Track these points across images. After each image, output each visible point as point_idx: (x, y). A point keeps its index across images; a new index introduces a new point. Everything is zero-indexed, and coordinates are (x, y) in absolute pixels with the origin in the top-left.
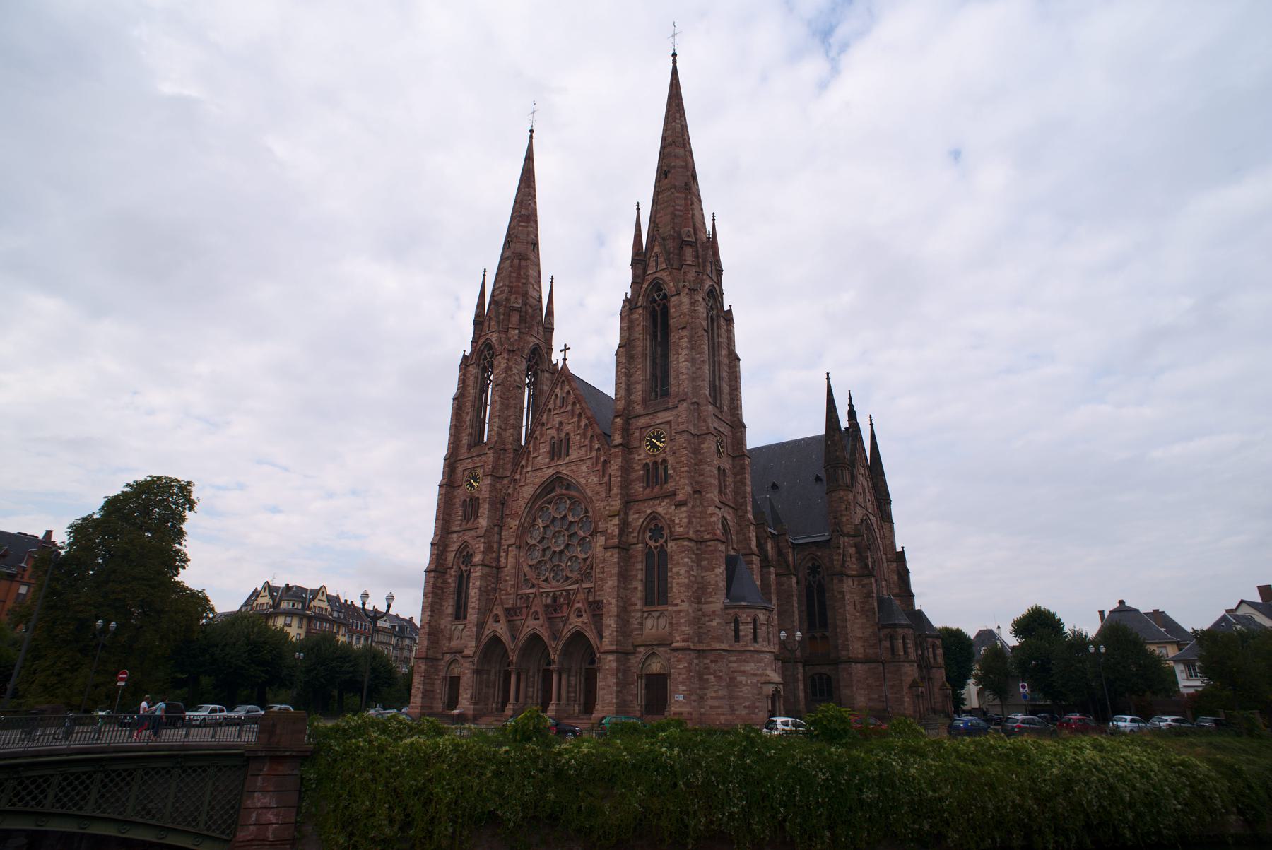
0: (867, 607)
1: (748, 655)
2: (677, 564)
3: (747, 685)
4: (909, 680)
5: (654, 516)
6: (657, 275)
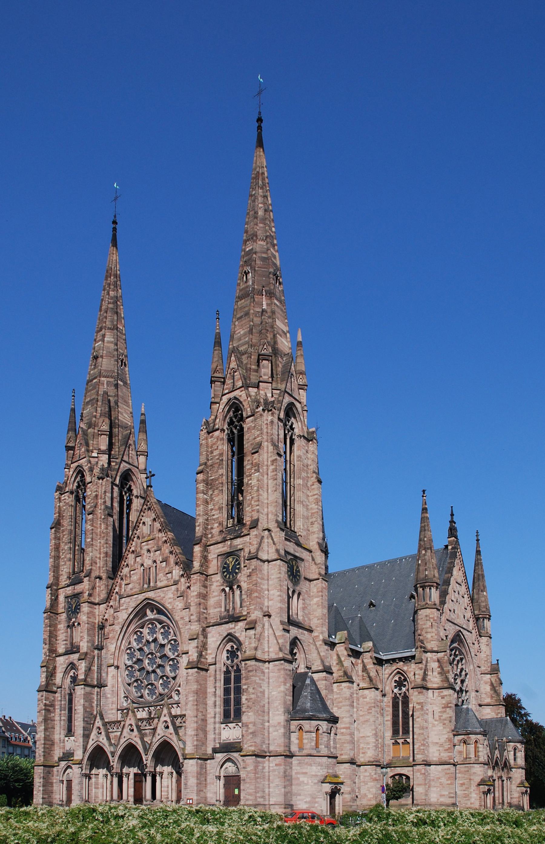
0: (445, 716)
4: (478, 779)
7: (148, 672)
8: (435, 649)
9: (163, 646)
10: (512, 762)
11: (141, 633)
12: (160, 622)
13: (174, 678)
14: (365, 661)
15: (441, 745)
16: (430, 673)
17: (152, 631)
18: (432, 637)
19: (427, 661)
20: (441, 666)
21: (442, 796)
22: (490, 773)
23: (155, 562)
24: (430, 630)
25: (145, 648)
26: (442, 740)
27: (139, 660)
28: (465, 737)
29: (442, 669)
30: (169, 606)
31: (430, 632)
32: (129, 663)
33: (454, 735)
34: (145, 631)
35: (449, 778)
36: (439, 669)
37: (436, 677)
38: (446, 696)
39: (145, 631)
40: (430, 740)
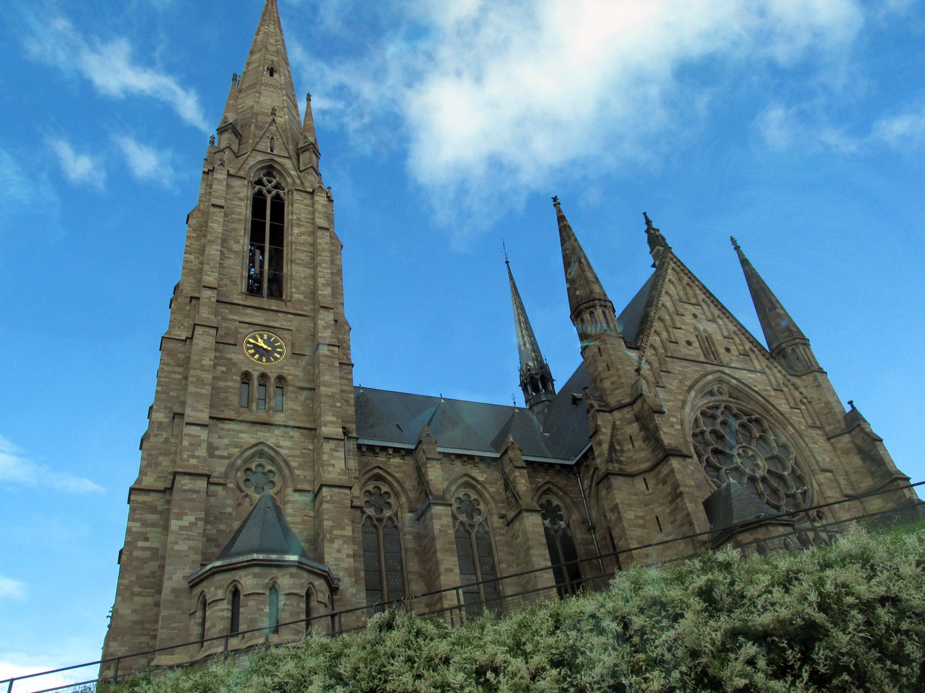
16: (627, 446)
18: (612, 383)
19: (614, 427)
31: (607, 378)
36: (643, 433)
37: (643, 450)
38: (667, 475)
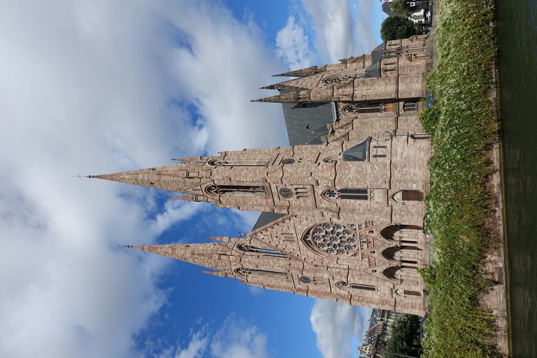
0: (369, 83)
1: (393, 151)
2: (347, 185)
3: (408, 152)
4: (408, 62)
5: (323, 194)
6: (203, 190)
7: (341, 242)
8: (332, 91)
9: (326, 232)
10: (398, 46)
11: (319, 244)
12: (314, 233)
13: (345, 227)
14: (337, 127)
15: (387, 84)
16: (345, 93)
17: (318, 238)
20: (341, 87)
21: (417, 82)
22: (404, 56)
23: (282, 234)
24: (321, 94)
25: (328, 243)
26: (384, 83)
27: (334, 247)
28: (382, 71)
29: (343, 86)
30: (306, 228)
32: (336, 251)
33: (381, 77)
34: (318, 242)
35: (407, 78)
39: (318, 242)
40: (383, 90)
